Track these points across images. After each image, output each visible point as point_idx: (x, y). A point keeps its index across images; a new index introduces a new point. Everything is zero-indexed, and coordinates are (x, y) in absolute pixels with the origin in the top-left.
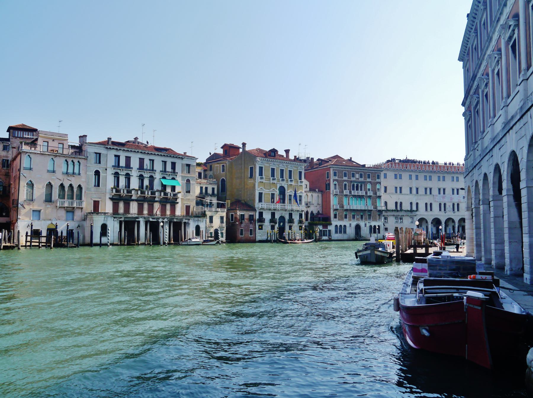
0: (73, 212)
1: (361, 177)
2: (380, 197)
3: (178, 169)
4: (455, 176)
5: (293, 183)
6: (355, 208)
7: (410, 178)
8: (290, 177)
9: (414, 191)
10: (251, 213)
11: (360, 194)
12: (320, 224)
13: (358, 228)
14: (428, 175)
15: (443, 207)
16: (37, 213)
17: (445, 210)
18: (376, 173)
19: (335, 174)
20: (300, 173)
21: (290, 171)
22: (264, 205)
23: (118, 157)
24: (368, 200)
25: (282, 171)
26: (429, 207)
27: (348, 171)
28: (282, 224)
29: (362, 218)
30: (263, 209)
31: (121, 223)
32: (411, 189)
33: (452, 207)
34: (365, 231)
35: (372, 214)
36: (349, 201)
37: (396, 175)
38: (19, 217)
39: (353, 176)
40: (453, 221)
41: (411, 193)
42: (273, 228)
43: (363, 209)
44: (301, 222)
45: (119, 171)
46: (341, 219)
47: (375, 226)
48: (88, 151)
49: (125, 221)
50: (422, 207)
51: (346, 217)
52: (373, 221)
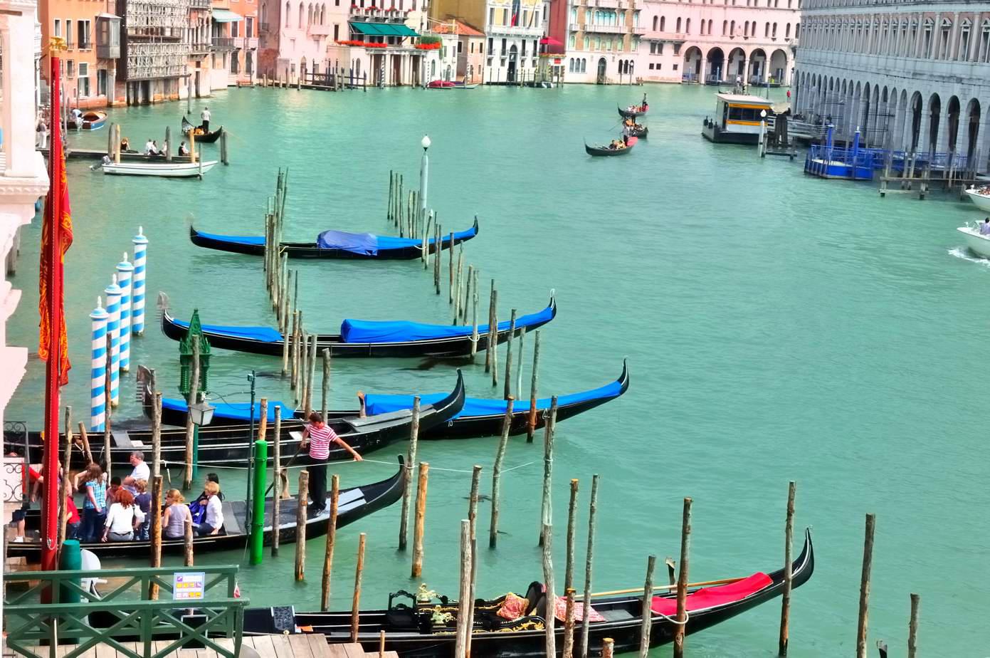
0: (318, 41)
10: (482, 40)
16: (292, 42)
17: (731, 33)
24: (621, 19)
26: (707, 25)
28: (513, 56)
30: (495, 34)
31: (371, 56)
33: (743, 27)
38: (280, 48)
42: (503, 61)
44: (535, 54)
47: (627, 62)
49: (375, 55)
50: (696, 26)
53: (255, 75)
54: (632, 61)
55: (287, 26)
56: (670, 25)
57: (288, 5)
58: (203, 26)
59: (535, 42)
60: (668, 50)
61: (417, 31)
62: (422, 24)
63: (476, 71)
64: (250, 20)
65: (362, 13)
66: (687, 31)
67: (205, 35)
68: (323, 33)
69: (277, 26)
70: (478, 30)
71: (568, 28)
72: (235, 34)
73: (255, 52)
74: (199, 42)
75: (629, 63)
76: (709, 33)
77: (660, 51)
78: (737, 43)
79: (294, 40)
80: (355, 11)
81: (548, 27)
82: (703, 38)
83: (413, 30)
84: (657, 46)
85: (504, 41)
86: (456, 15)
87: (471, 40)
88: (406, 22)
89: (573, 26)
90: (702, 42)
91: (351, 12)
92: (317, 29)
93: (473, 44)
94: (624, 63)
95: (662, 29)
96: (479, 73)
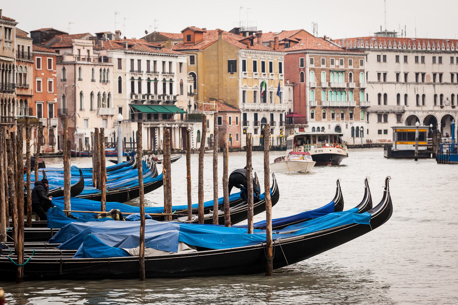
0: (106, 120)
1: (342, 64)
2: (363, 90)
3: (175, 69)
5: (274, 77)
6: (335, 105)
8: (271, 71)
9: (402, 79)
10: (237, 115)
12: (297, 127)
15: (439, 99)
16: (86, 121)
19: (312, 63)
20: (280, 64)
21: (271, 63)
22: (248, 106)
23: (132, 60)
24: (350, 93)
25: (263, 63)
26: (421, 99)
27: (326, 57)
29: (342, 117)
30: (248, 110)
32: (398, 75)
33: (450, 99)
35: (354, 113)
36: (327, 95)
37: (379, 57)
38: (77, 126)
39: (332, 63)
43: (345, 105)
44: (281, 124)
45: (134, 76)
46: (319, 120)
47: (358, 128)
48: (114, 57)
49: (151, 128)
50: (412, 100)
51: (324, 117)
52: (356, 120)
53: (56, 147)
54: (362, 127)
55: (81, 109)
56: (392, 101)
57: (81, 94)
58: (9, 104)
59: (281, 115)
60: (392, 119)
61: (185, 110)
62: (190, 106)
63: (234, 138)
64: (51, 106)
65: (140, 98)
67: (12, 110)
68: (110, 113)
69: (73, 110)
70: (235, 108)
71: (308, 104)
72: (40, 116)
73: (57, 128)
74: (7, 115)
75: (360, 128)
76: (423, 104)
77: (386, 121)
78: (446, 111)
79: (87, 120)
80: (134, 97)
81: (293, 105)
82: (419, 109)
83: (183, 109)
84: (382, 116)
85: (256, 115)
86: (217, 98)
87: (229, 115)
88: (176, 104)
89: (312, 102)
90: (418, 111)
91: (132, 97)
92: (104, 111)
93: (230, 118)
94: (355, 129)
95: (385, 103)
96: (237, 140)
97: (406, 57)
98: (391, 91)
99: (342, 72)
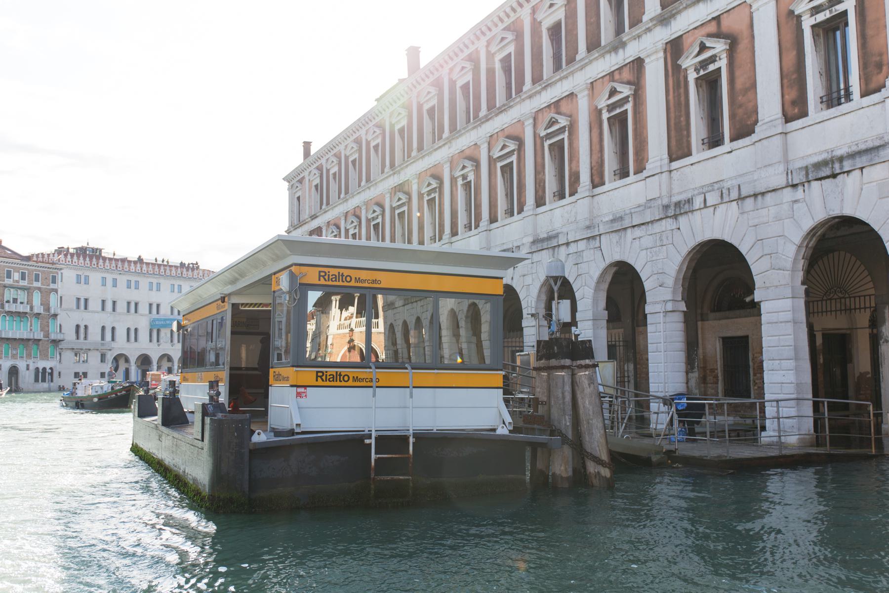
1: (23, 278)
4: (177, 283)
6: (10, 336)
7: (104, 285)
9: (109, 306)
11: (21, 310)
13: (14, 372)
14: (133, 279)
17: (158, 341)
18: (51, 272)
24: (34, 320)
26: (132, 334)
32: (103, 302)
33: (169, 335)
34: (26, 377)
37: (79, 276)
39: (9, 276)
40: (170, 359)
41: (103, 309)
43: (25, 337)
50: (121, 334)
52: (42, 359)
56: (94, 335)
66: (113, 339)
95: (86, 338)
97: (115, 280)
98: (95, 320)
99: (23, 289)
